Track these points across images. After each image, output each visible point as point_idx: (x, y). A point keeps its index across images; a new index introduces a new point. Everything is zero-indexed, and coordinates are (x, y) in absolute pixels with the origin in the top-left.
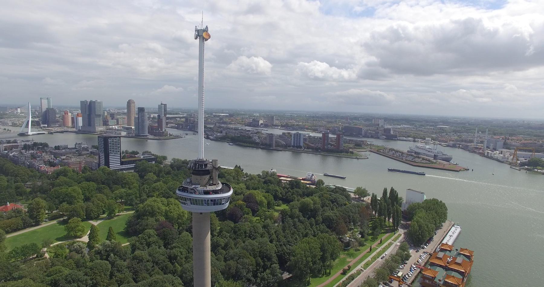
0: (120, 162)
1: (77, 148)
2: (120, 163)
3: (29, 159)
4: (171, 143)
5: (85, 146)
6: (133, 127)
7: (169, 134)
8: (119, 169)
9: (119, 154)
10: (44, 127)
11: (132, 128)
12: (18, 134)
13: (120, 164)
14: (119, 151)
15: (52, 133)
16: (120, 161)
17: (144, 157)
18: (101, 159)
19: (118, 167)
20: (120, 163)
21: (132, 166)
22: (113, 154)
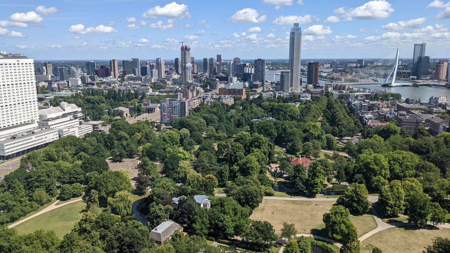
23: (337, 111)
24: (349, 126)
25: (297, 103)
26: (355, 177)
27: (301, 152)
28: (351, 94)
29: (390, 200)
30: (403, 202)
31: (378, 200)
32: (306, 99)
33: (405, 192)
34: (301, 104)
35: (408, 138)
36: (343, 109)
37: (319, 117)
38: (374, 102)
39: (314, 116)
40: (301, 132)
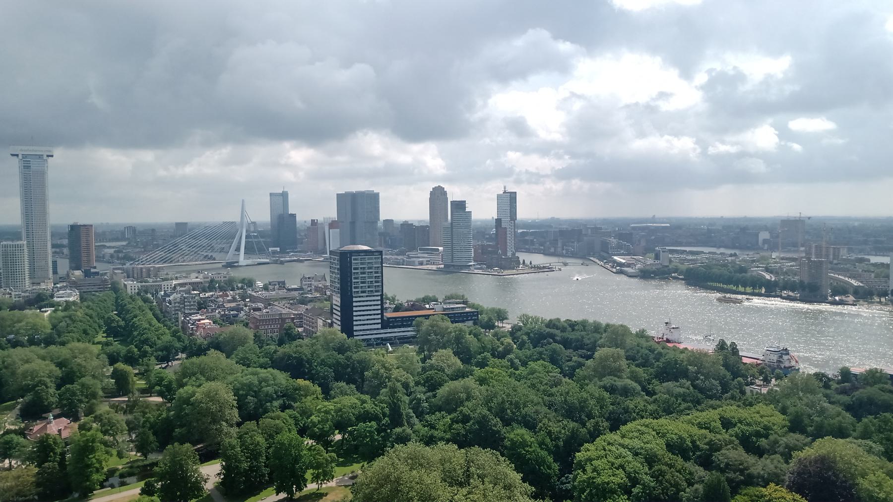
0: (382, 318)
1: (304, 287)
2: (380, 321)
3: (192, 309)
4: (523, 278)
5: (320, 282)
6: (441, 248)
7: (521, 262)
8: (378, 339)
9: (379, 298)
10: (274, 252)
11: (438, 249)
12: (225, 264)
13: (379, 326)
14: (376, 291)
15: (282, 263)
16: (379, 316)
17: (445, 310)
18: (334, 311)
19: (375, 332)
20: (380, 321)
21: (409, 332)
22: (362, 297)
23: (135, 316)
24: (160, 342)
25: (47, 309)
26: (174, 434)
27: (57, 411)
28: (163, 283)
29: (240, 462)
30: (263, 459)
31: (220, 468)
32: (67, 299)
33: (266, 440)
34: (55, 311)
35: (268, 347)
36: (148, 311)
37: (97, 333)
38: (207, 295)
39: (85, 332)
40: (53, 367)
